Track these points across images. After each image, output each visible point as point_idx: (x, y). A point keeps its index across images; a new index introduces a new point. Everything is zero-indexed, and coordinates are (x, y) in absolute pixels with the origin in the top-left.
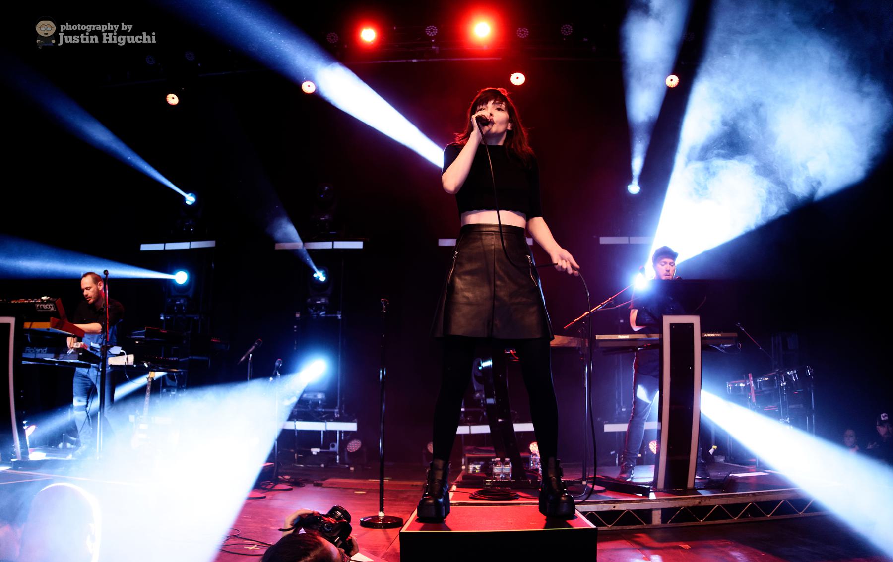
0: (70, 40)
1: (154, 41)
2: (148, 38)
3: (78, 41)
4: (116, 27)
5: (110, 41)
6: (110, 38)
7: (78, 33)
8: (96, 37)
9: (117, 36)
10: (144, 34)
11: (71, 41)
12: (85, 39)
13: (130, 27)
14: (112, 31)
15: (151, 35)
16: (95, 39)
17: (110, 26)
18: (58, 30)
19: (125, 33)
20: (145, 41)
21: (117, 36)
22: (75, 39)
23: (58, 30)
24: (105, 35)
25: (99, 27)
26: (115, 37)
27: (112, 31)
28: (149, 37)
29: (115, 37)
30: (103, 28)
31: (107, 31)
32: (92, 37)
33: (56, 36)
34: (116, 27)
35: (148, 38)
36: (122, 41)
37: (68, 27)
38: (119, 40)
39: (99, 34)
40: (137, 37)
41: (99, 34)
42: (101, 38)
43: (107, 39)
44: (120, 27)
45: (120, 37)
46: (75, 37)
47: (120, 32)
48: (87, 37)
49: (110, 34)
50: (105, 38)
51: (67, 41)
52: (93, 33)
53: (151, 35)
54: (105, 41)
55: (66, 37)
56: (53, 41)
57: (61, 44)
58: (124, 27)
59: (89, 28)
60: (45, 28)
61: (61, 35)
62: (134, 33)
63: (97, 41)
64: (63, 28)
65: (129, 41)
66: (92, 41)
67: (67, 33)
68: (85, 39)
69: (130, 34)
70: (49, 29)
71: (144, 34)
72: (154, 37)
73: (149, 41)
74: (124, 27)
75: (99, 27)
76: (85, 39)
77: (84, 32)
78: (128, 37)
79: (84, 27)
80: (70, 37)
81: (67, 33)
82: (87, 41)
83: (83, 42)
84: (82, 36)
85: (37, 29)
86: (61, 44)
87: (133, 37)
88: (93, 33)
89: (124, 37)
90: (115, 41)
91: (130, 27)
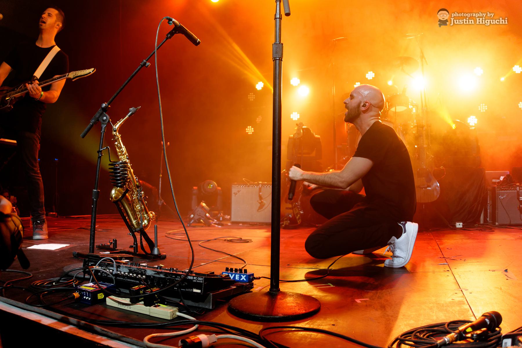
1: (506, 23)
6: (481, 21)
8: (473, 21)
10: (501, 19)
12: (466, 22)
14: (482, 17)
15: (505, 20)
17: (481, 15)
20: (501, 23)
24: (478, 19)
26: (484, 21)
27: (482, 17)
29: (484, 21)
32: (470, 21)
37: (456, 15)
38: (486, 22)
48: (467, 21)
49: (481, 19)
50: (478, 21)
53: (505, 20)
54: (477, 23)
61: (452, 19)
71: (501, 19)
72: (506, 21)
76: (466, 22)
78: (491, 21)
79: (465, 15)
80: (458, 21)
84: (465, 20)
89: (489, 21)
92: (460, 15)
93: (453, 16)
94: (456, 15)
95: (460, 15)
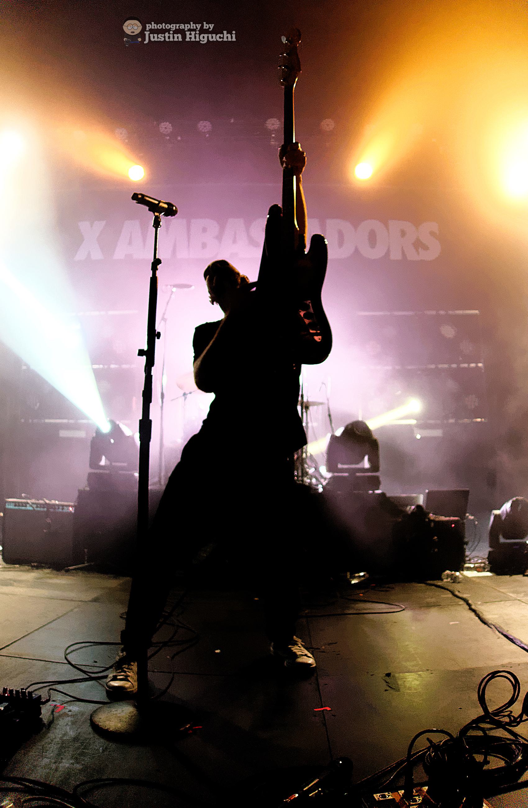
0: (155, 38)
1: (234, 39)
2: (228, 37)
3: (163, 39)
4: (199, 26)
5: (193, 39)
6: (193, 36)
7: (163, 31)
8: (180, 35)
9: (200, 34)
10: (225, 32)
11: (156, 39)
12: (169, 37)
13: (212, 26)
14: (194, 30)
15: (231, 34)
16: (178, 37)
17: (192, 26)
18: (144, 29)
19: (207, 31)
20: (225, 39)
21: (200, 34)
22: (160, 38)
23: (144, 29)
24: (188, 33)
25: (182, 26)
26: (197, 36)
27: (194, 30)
28: (229, 35)
29: (197, 36)
30: (187, 27)
31: (190, 30)
32: (176, 36)
33: (142, 34)
34: (199, 26)
35: (228, 37)
36: (204, 39)
37: (153, 26)
39: (183, 32)
40: (218, 35)
41: (183, 32)
42: (184, 37)
43: (191, 37)
44: (203, 26)
45: (202, 36)
46: (159, 35)
47: (203, 31)
48: (171, 36)
49: (193, 33)
51: (152, 39)
52: (176, 31)
53: (231, 34)
54: (188, 39)
55: (151, 35)
56: (140, 40)
57: (147, 41)
58: (206, 26)
59: (173, 27)
60: (132, 27)
61: (147, 33)
62: (215, 31)
63: (180, 39)
64: (148, 26)
65: (211, 39)
66: (176, 39)
67: (152, 31)
68: (169, 37)
69: (212, 33)
70: (136, 28)
71: (225, 32)
72: (234, 36)
73: (230, 39)
74: (206, 26)
75: (182, 26)
76: (169, 37)
77: (168, 31)
78: (210, 35)
79: (168, 26)
80: (156, 35)
81: (152, 31)
82: (171, 39)
83: (167, 40)
85: (124, 28)
86: (147, 41)
87: (214, 35)
88: (176, 31)
89: (206, 36)
90: (197, 39)
91: (212, 26)
92: (160, 26)
93: (147, 29)
94: (153, 26)
95: (160, 26)
